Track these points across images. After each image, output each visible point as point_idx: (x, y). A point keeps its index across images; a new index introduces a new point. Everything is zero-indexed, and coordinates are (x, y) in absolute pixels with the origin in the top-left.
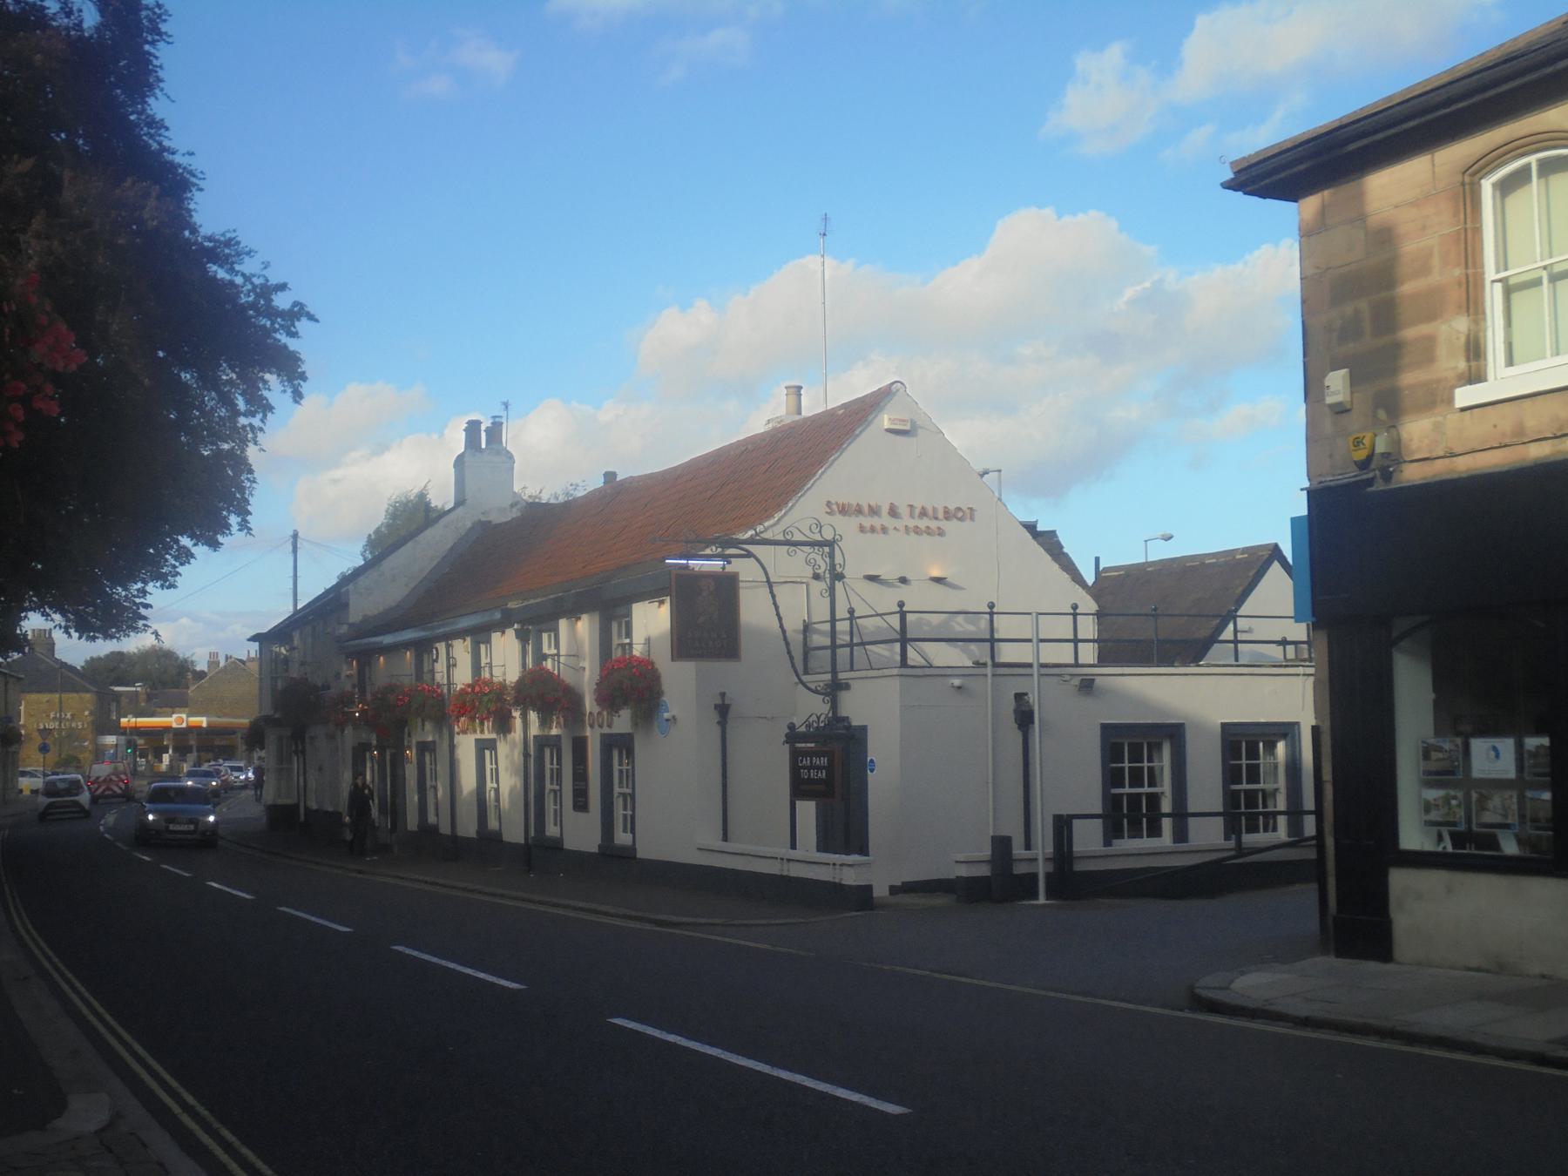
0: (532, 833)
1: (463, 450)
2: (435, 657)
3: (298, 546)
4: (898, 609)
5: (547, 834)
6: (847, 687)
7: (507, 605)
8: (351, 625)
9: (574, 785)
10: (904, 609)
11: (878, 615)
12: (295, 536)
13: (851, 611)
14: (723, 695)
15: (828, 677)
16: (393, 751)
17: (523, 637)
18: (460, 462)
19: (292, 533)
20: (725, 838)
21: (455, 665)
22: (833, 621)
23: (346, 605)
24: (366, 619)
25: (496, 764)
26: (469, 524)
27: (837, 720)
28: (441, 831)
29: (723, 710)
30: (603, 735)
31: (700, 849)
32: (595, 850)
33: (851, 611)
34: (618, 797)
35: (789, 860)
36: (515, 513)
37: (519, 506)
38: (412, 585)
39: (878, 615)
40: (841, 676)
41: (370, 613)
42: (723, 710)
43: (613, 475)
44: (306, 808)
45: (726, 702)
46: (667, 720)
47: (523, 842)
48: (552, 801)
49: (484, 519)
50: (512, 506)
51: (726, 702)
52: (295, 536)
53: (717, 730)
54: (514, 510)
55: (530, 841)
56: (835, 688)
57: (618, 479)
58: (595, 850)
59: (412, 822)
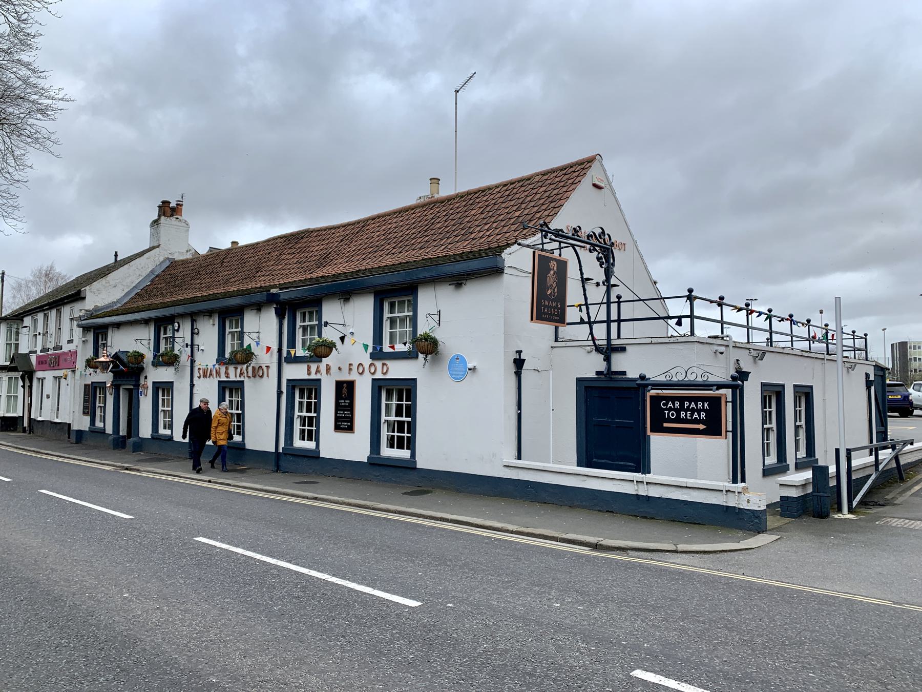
0: (282, 444)
1: (156, 217)
2: (176, 328)
3: (5, 279)
4: (688, 293)
5: (294, 445)
6: (622, 349)
7: (270, 291)
8: (86, 311)
9: (336, 413)
10: (693, 294)
11: (643, 300)
12: (3, 274)
13: (619, 297)
14: (519, 352)
15: (605, 342)
16: (132, 387)
17: (280, 315)
18: (156, 223)
19: (1, 272)
20: (519, 457)
21: (197, 334)
22: (609, 303)
23: (84, 298)
24: (97, 309)
25: (796, 412)
26: (162, 259)
27: (609, 374)
28: (107, 432)
29: (519, 363)
30: (374, 380)
31: (505, 466)
32: (366, 460)
33: (619, 297)
34: (384, 423)
35: (647, 483)
36: (189, 256)
37: (191, 252)
38: (126, 290)
39: (640, 300)
40: (613, 342)
41: (99, 305)
42: (519, 363)
43: (237, 243)
44: (30, 419)
45: (522, 358)
46: (470, 369)
47: (273, 450)
48: (99, 411)
49: (170, 257)
50: (187, 251)
51: (522, 358)
52: (3, 274)
53: (513, 378)
54: (189, 253)
55: (281, 450)
56: (608, 350)
57: (239, 245)
58: (366, 460)
59: (145, 431)
